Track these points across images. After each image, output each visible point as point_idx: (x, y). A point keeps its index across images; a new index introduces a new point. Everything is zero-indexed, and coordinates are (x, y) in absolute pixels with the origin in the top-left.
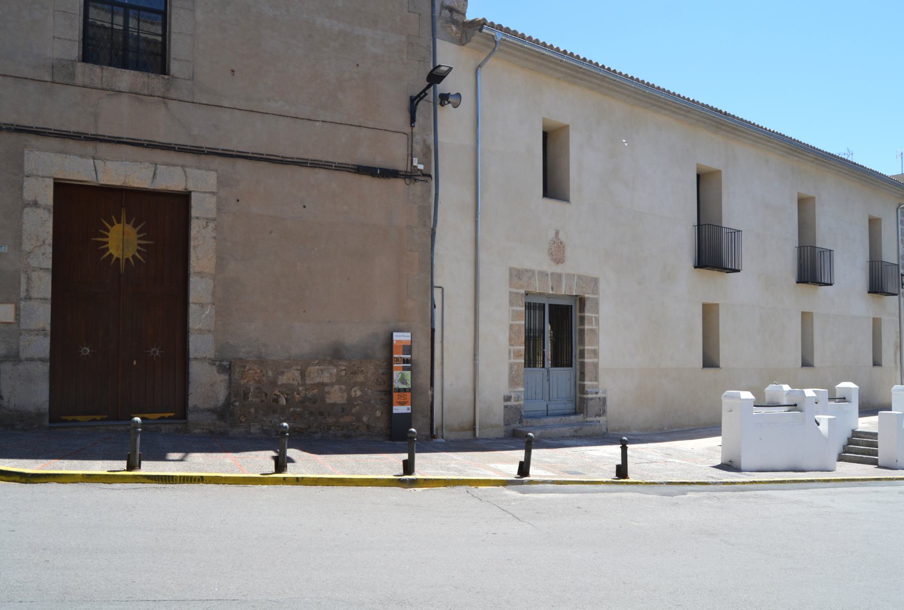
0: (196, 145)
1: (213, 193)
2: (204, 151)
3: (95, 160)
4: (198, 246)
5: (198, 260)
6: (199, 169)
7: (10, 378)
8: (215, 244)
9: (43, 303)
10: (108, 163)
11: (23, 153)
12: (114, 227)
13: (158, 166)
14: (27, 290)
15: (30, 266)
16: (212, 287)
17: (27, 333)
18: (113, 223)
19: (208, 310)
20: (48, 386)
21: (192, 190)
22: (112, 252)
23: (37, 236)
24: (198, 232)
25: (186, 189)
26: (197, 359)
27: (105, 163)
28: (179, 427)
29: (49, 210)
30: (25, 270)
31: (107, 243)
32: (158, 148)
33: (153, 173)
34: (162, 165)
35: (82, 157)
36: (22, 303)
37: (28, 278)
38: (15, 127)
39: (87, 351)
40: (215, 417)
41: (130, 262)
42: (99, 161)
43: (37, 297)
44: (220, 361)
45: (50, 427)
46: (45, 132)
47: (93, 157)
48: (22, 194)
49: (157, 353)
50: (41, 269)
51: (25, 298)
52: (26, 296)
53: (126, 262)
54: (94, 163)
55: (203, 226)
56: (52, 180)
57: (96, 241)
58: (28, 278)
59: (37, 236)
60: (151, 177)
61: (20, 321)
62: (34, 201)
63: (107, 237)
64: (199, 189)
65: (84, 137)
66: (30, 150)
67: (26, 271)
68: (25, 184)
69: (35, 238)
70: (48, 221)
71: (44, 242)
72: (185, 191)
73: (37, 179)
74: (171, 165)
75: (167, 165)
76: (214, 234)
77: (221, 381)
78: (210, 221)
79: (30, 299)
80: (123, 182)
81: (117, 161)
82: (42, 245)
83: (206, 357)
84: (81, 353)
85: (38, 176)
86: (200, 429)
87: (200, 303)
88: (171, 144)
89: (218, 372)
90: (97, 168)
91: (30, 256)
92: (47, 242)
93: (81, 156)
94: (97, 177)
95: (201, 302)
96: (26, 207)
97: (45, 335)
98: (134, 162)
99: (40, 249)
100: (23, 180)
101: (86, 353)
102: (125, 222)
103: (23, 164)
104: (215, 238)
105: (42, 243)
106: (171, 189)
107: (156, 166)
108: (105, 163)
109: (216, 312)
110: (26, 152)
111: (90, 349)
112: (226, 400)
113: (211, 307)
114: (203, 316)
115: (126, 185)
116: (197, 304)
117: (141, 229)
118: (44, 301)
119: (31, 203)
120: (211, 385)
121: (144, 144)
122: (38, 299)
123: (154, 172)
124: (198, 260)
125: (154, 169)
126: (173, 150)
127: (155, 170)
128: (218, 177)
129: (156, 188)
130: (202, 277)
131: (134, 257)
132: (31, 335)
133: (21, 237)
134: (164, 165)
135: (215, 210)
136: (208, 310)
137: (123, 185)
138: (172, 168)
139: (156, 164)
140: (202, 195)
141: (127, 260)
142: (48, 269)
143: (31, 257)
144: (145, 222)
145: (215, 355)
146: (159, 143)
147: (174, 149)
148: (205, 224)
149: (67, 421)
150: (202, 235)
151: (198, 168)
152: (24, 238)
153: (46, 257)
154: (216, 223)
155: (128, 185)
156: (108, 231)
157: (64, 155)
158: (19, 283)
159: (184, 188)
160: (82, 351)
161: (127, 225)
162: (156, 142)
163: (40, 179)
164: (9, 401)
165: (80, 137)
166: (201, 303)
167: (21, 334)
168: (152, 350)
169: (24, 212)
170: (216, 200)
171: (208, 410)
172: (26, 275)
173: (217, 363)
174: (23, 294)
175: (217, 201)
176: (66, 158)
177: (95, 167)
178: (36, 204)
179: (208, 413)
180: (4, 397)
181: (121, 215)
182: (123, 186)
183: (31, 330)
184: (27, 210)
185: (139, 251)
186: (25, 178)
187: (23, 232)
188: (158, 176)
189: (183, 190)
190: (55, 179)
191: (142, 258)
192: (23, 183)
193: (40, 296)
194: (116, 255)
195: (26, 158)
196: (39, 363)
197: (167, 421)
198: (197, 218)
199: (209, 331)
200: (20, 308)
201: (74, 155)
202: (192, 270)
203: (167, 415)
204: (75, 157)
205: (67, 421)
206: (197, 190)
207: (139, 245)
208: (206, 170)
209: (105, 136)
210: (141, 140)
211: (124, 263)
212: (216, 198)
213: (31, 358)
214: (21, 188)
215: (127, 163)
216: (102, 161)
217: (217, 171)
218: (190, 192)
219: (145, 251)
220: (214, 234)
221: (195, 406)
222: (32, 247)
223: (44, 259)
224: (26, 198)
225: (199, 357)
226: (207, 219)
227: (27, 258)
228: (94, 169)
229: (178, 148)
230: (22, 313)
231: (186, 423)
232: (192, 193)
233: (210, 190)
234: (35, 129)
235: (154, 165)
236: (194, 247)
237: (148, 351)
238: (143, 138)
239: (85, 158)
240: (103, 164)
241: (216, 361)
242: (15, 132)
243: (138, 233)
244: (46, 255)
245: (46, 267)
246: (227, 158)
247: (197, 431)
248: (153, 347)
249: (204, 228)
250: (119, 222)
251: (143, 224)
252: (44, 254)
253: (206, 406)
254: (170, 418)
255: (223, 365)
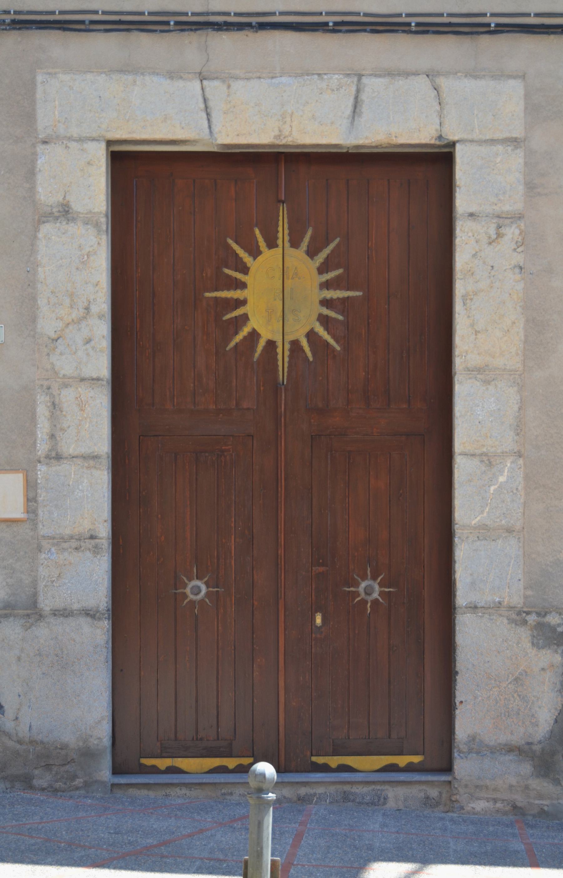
0: (464, 10)
1: (514, 142)
2: (489, 25)
3: (205, 83)
4: (475, 294)
5: (477, 332)
6: (476, 77)
7: (19, 659)
8: (520, 286)
9: (88, 468)
10: (237, 85)
11: (33, 82)
12: (260, 258)
13: (365, 80)
14: (52, 436)
15: (56, 373)
16: (516, 408)
17: (54, 545)
18: (258, 247)
19: (506, 474)
20: (108, 681)
21: (456, 138)
22: (256, 328)
23: (72, 295)
24: (474, 256)
25: (440, 137)
26: (476, 607)
27: (229, 87)
28: (434, 793)
29: (97, 225)
30: (46, 383)
31: (243, 303)
32: (365, 31)
33: (350, 102)
34: (376, 76)
35: (171, 78)
36: (42, 470)
37: (54, 404)
38: (13, 17)
39: (200, 591)
40: (526, 768)
41: (301, 349)
42: (216, 83)
43: (76, 453)
44: (538, 614)
45: (113, 785)
46: (82, 22)
47: (200, 73)
48: (32, 189)
49: (376, 595)
50: (83, 380)
51: (48, 457)
52: (50, 451)
53: (292, 351)
54: (203, 89)
55: (490, 238)
56: (103, 145)
57: (216, 298)
58: (54, 404)
59: (72, 295)
60: (349, 111)
61: (37, 515)
62: (62, 205)
63: (243, 286)
64: (476, 135)
65: (177, 23)
66: (49, 74)
67: (49, 388)
68: (39, 162)
69: (67, 301)
70: (95, 253)
71: (87, 309)
72: (438, 143)
73: (67, 147)
74: (399, 75)
75: (390, 74)
76: (519, 259)
77: (543, 669)
78: (507, 221)
79: (59, 457)
80: (277, 133)
81: (260, 78)
82: (85, 318)
83: (500, 603)
84: (185, 596)
85: (70, 139)
86: (488, 800)
87: (481, 455)
88: (400, 15)
89: (533, 644)
90: (211, 104)
91: (55, 349)
92: (94, 309)
93: (172, 75)
94: (210, 127)
95: (485, 450)
96: (44, 222)
97: (96, 550)
98: (302, 75)
99: (79, 330)
100: (35, 154)
101: (197, 594)
102: (287, 244)
103: (34, 110)
104: (521, 268)
105: (82, 311)
106: (402, 140)
107: (359, 80)
108: (229, 87)
109: (527, 478)
110: (40, 78)
111: (207, 584)
112: (556, 721)
113: (512, 462)
114: (492, 488)
115: (284, 142)
116: (473, 455)
117: (327, 259)
118: (92, 463)
119: (55, 210)
120: (516, 679)
121: (326, 24)
122: (76, 457)
123: (356, 98)
124: (477, 332)
125: (354, 89)
126: (404, 31)
127: (358, 91)
128: (527, 96)
129: (361, 142)
130: (487, 382)
131: (311, 335)
132: (64, 549)
133: (34, 299)
134: (380, 76)
135: (521, 188)
136: (506, 474)
137: (278, 142)
138: (401, 82)
139: (360, 76)
140: (484, 150)
141: (295, 345)
142: (98, 379)
143: (58, 351)
144: (338, 240)
145: (526, 597)
146: (366, 15)
147: (406, 28)
148: (492, 232)
149: (154, 770)
150: (484, 263)
151: (473, 74)
152: (42, 302)
153: (93, 348)
154: (523, 228)
155: (289, 141)
156: (245, 270)
157: (130, 78)
158: (33, 418)
159: (435, 134)
160: (188, 591)
161: (290, 251)
162: (358, 14)
163: (73, 145)
164: (17, 718)
165: (167, 23)
166: (486, 455)
167: (40, 549)
168: (363, 585)
169: (40, 235)
170: (521, 161)
171: (510, 749)
172: (48, 398)
173: (532, 619)
174: (42, 448)
175: (526, 163)
176: (135, 82)
177: (205, 100)
178: (67, 212)
179: (510, 757)
180: (6, 707)
181: (277, 226)
182: (279, 146)
183: (63, 539)
184: (46, 229)
185: (324, 320)
186: (40, 148)
187: (39, 286)
188: (365, 109)
189: (433, 142)
190: (109, 143)
191: (334, 337)
192: (34, 162)
193: (83, 450)
194: (266, 335)
195: (39, 95)
196: (83, 621)
197: (402, 777)
198: (471, 215)
199: (509, 530)
200: (36, 484)
201: (154, 73)
202: (459, 363)
203: (402, 761)
204: (155, 79)
205: (154, 770)
206: (470, 137)
207: (326, 303)
208: (494, 77)
209: (228, 14)
210: (321, 14)
211: (287, 353)
212: (522, 154)
213: (65, 609)
214: (31, 174)
215: (284, 79)
216: (224, 81)
217: (523, 77)
218: (453, 144)
219: (340, 318)
220: (519, 259)
221: (473, 738)
222: (60, 324)
223: (88, 354)
224: (42, 198)
225: (482, 604)
226: (499, 217)
227: (48, 355)
228: (202, 106)
229: (418, 24)
230: (42, 496)
231: (450, 782)
232: (458, 147)
233: (506, 135)
234: (58, 17)
235: (355, 79)
236: (465, 298)
237: (352, 589)
238: (323, 7)
239: (181, 78)
240: (225, 88)
241: (528, 613)
242: (14, 29)
243: (322, 270)
244: (92, 343)
245: (95, 376)
246: (552, 37)
247: (480, 806)
248: (364, 578)
249: (490, 243)
250: (272, 244)
251: (332, 246)
252: (88, 341)
253: (503, 738)
254: (410, 768)
255: (549, 625)
